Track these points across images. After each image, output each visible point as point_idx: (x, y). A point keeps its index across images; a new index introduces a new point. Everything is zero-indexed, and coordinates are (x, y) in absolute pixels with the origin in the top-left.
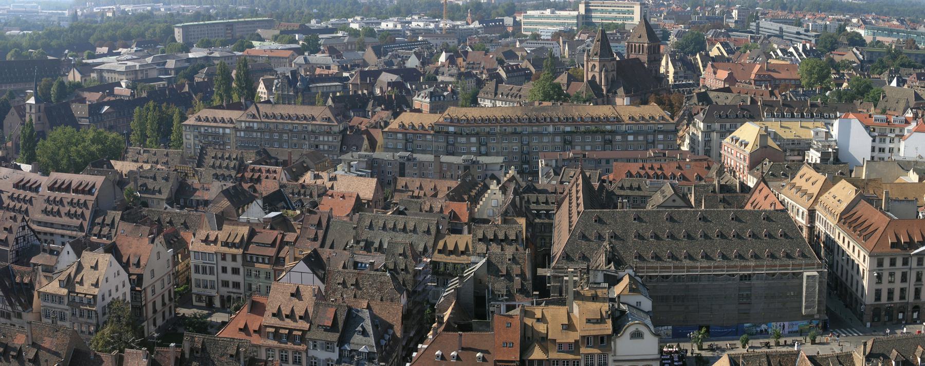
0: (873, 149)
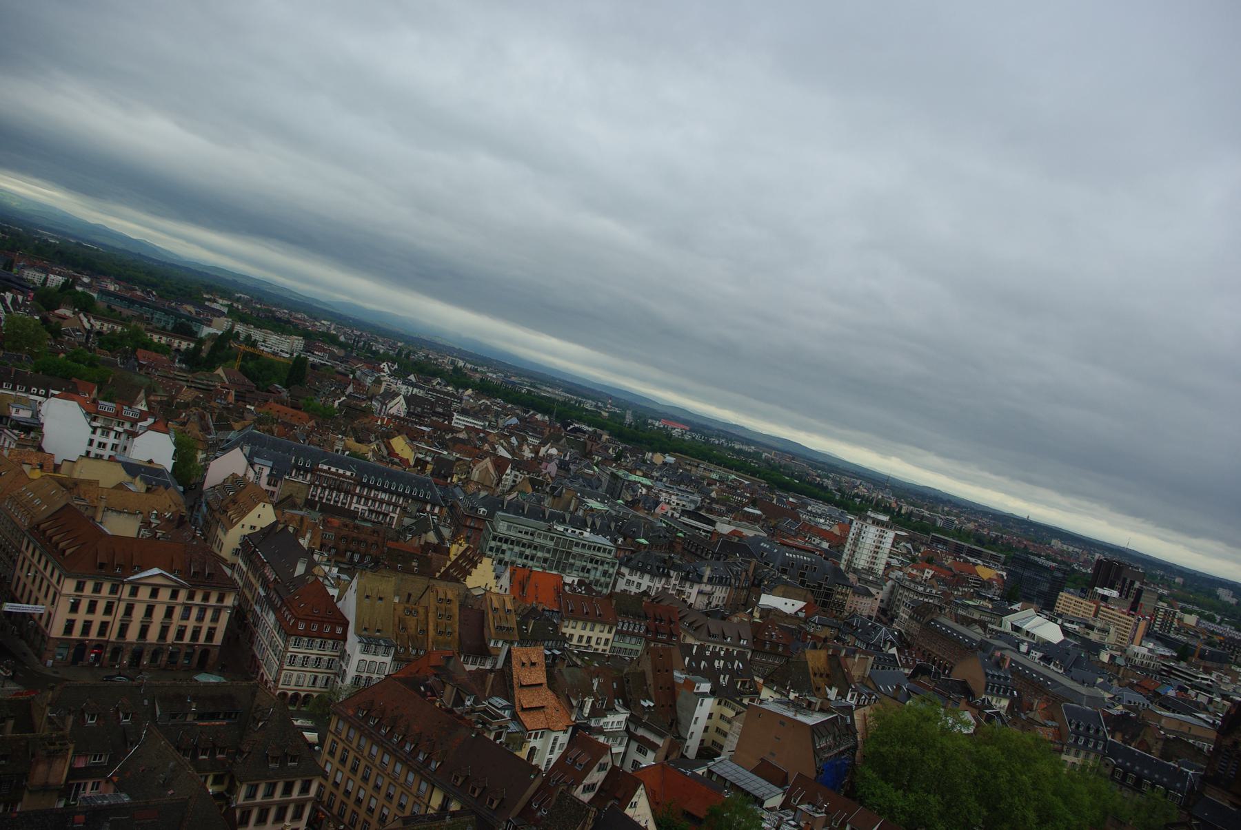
0: (91, 442)
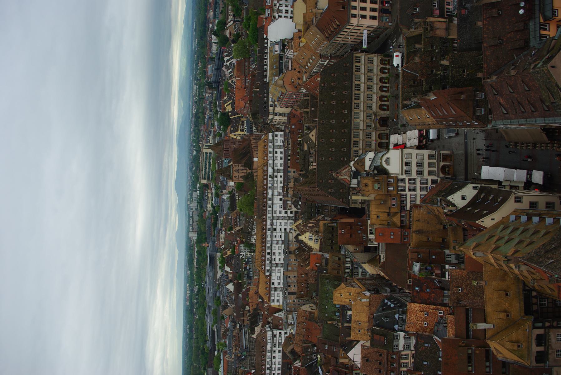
0: (286, 17)
